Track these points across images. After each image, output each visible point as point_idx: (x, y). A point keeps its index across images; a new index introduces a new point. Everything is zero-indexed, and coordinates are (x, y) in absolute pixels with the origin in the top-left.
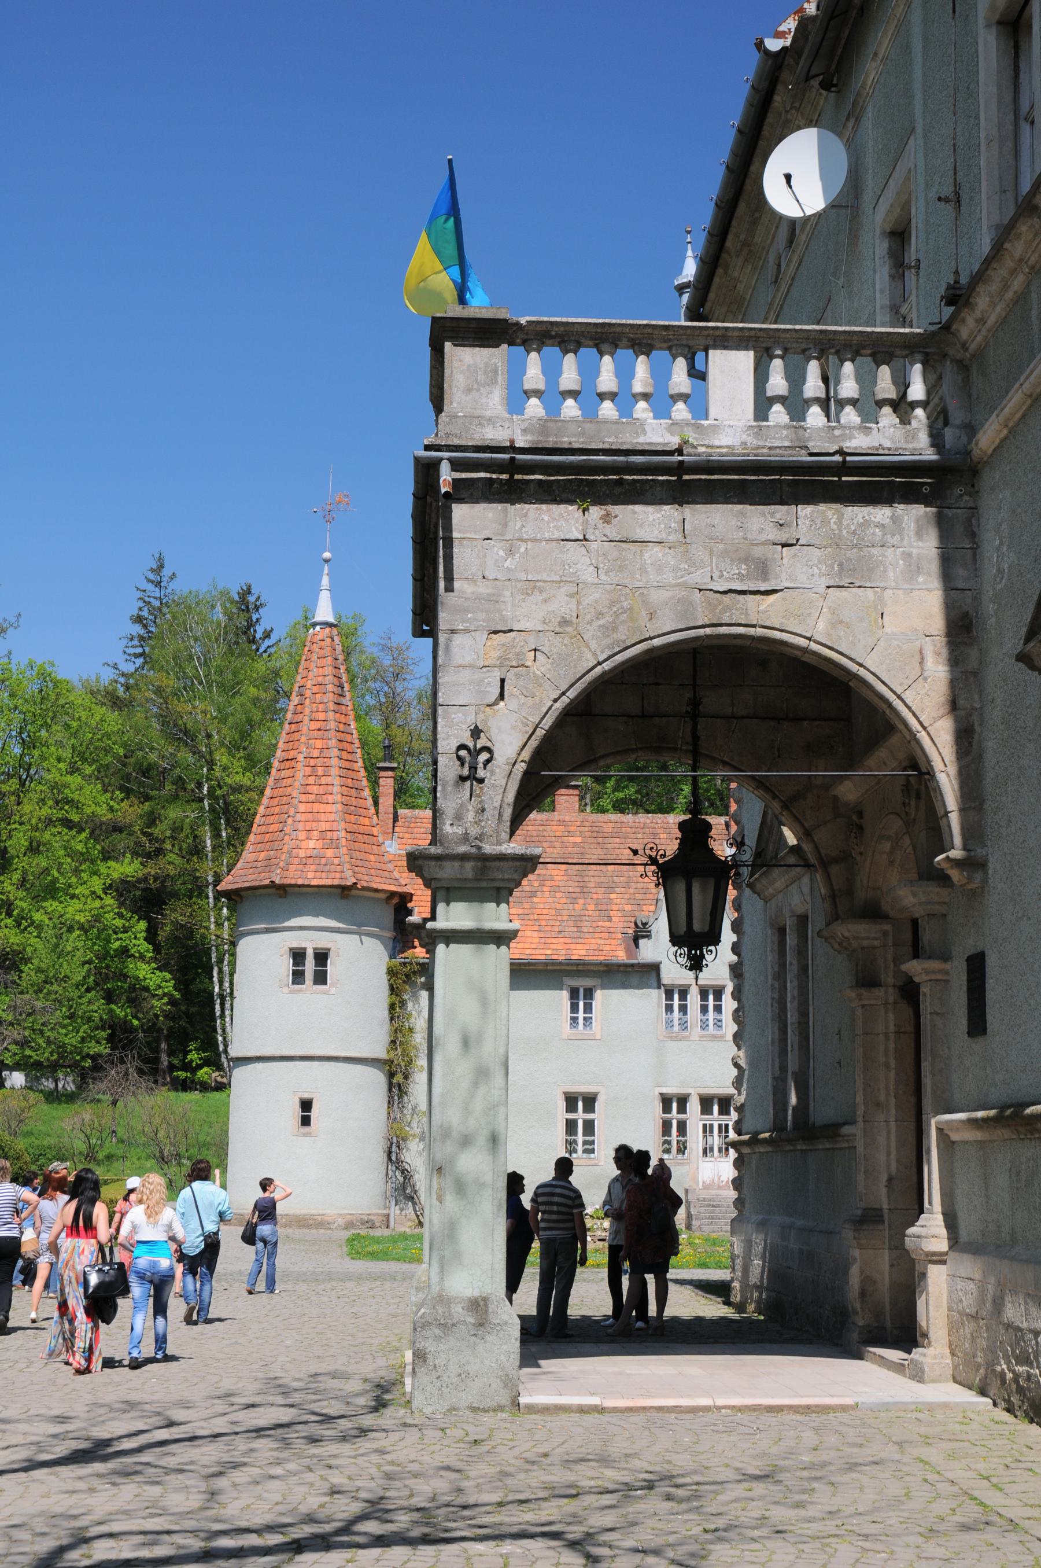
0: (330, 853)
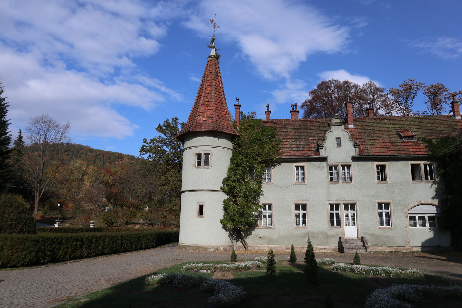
0: (210, 121)
